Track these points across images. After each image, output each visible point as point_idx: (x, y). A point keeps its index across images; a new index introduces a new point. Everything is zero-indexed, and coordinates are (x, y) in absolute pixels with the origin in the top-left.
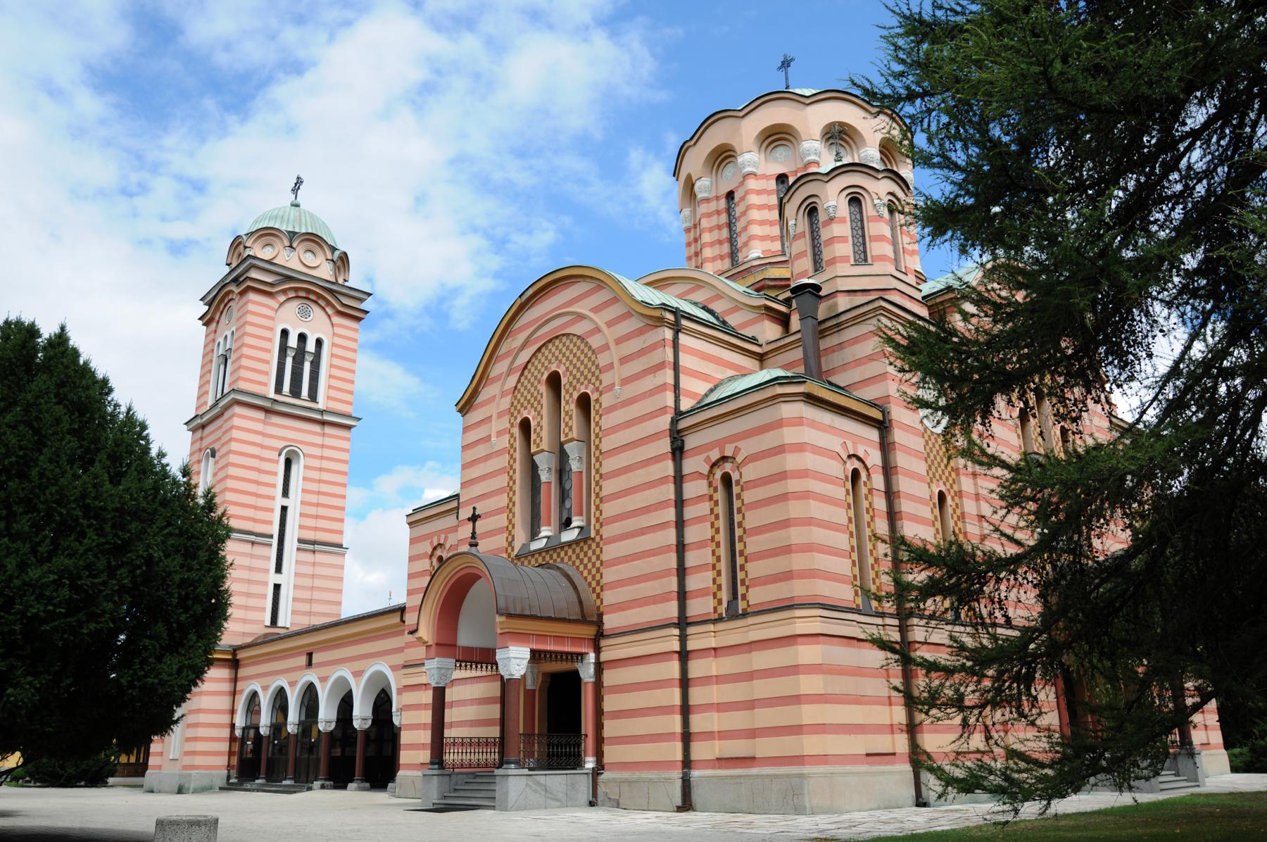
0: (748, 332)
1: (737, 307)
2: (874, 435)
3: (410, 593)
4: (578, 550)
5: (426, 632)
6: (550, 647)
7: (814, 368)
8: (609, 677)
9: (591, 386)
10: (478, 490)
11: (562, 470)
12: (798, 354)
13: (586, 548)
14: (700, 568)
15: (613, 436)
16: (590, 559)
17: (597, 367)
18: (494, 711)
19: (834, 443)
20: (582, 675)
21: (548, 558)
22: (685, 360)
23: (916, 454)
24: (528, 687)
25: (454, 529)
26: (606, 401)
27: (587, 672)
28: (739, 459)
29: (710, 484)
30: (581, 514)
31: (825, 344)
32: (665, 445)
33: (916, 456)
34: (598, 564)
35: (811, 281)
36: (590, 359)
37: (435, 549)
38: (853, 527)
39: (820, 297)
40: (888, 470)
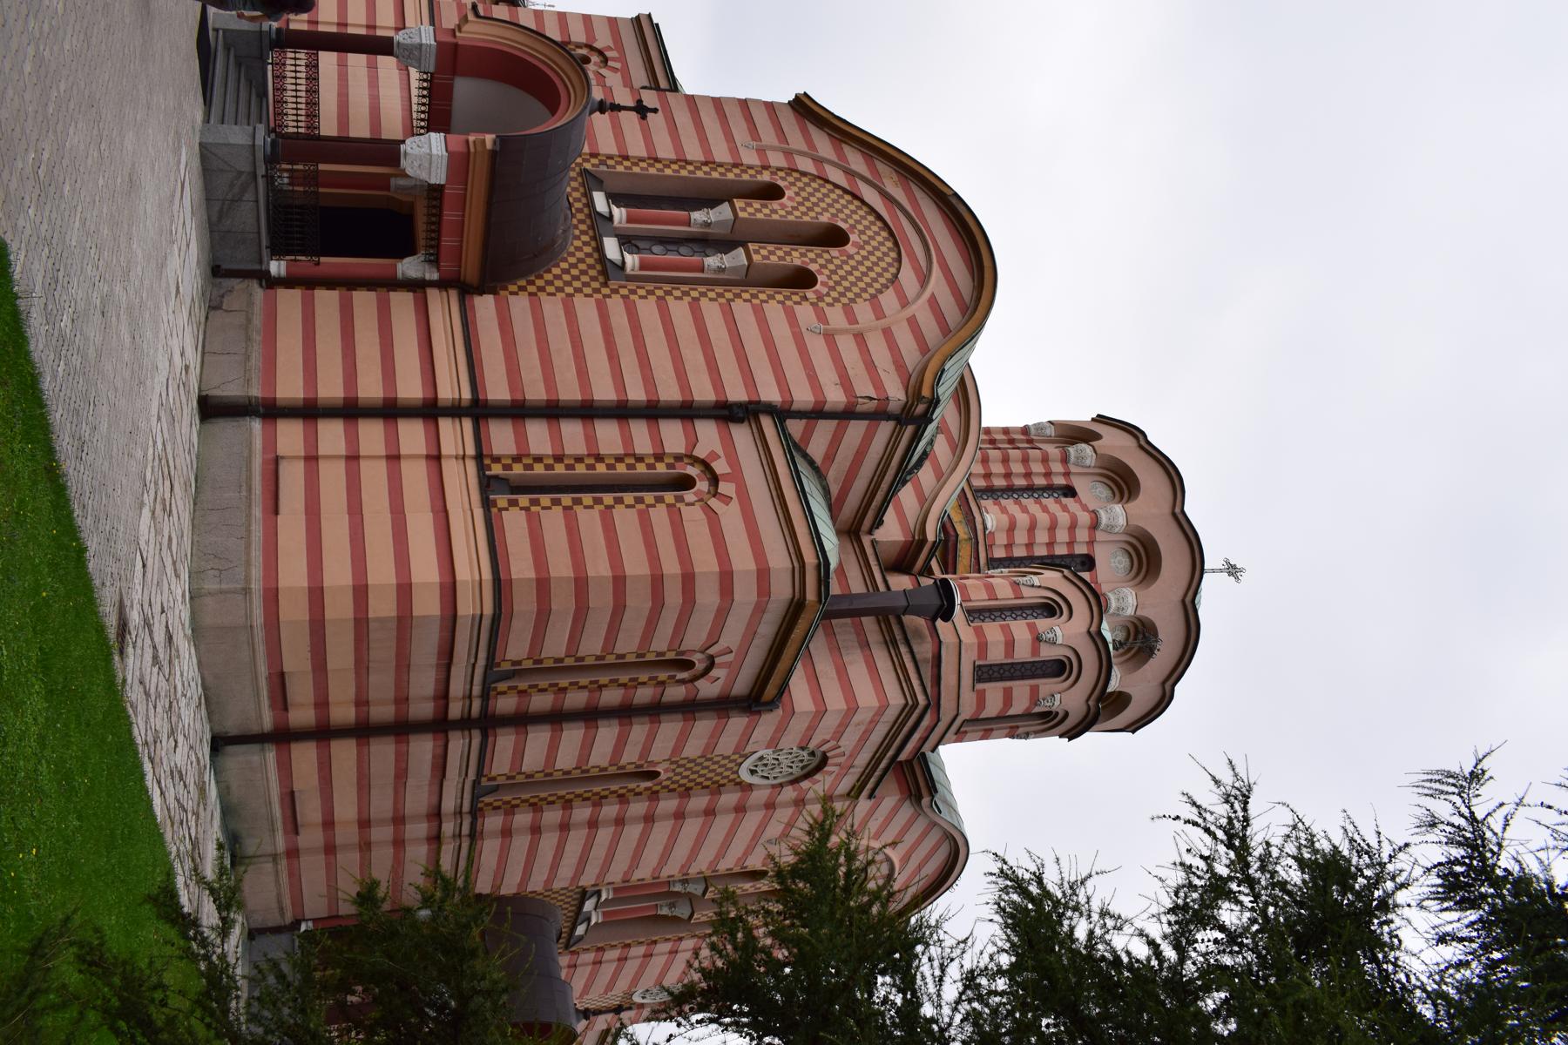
0: (890, 516)
1: (925, 503)
2: (741, 687)
3: (539, 15)
4: (590, 261)
5: (475, 33)
6: (449, 215)
7: (838, 610)
8: (402, 302)
9: (825, 291)
10: (683, 118)
11: (708, 242)
12: (857, 586)
13: (593, 273)
14: (557, 438)
15: (752, 319)
16: (576, 278)
17: (853, 301)
18: (360, 129)
19: (732, 636)
20: (407, 260)
21: (580, 216)
22: (856, 429)
23: (711, 745)
24: (393, 181)
25: (627, 82)
26: (805, 313)
27: (410, 267)
28: (713, 503)
29: (678, 458)
30: (642, 268)
31: (869, 622)
32: (736, 393)
33: (707, 745)
34: (569, 290)
35: (957, 608)
36: (864, 290)
37: (600, 53)
38: (610, 659)
39: (934, 620)
40: (690, 708)
